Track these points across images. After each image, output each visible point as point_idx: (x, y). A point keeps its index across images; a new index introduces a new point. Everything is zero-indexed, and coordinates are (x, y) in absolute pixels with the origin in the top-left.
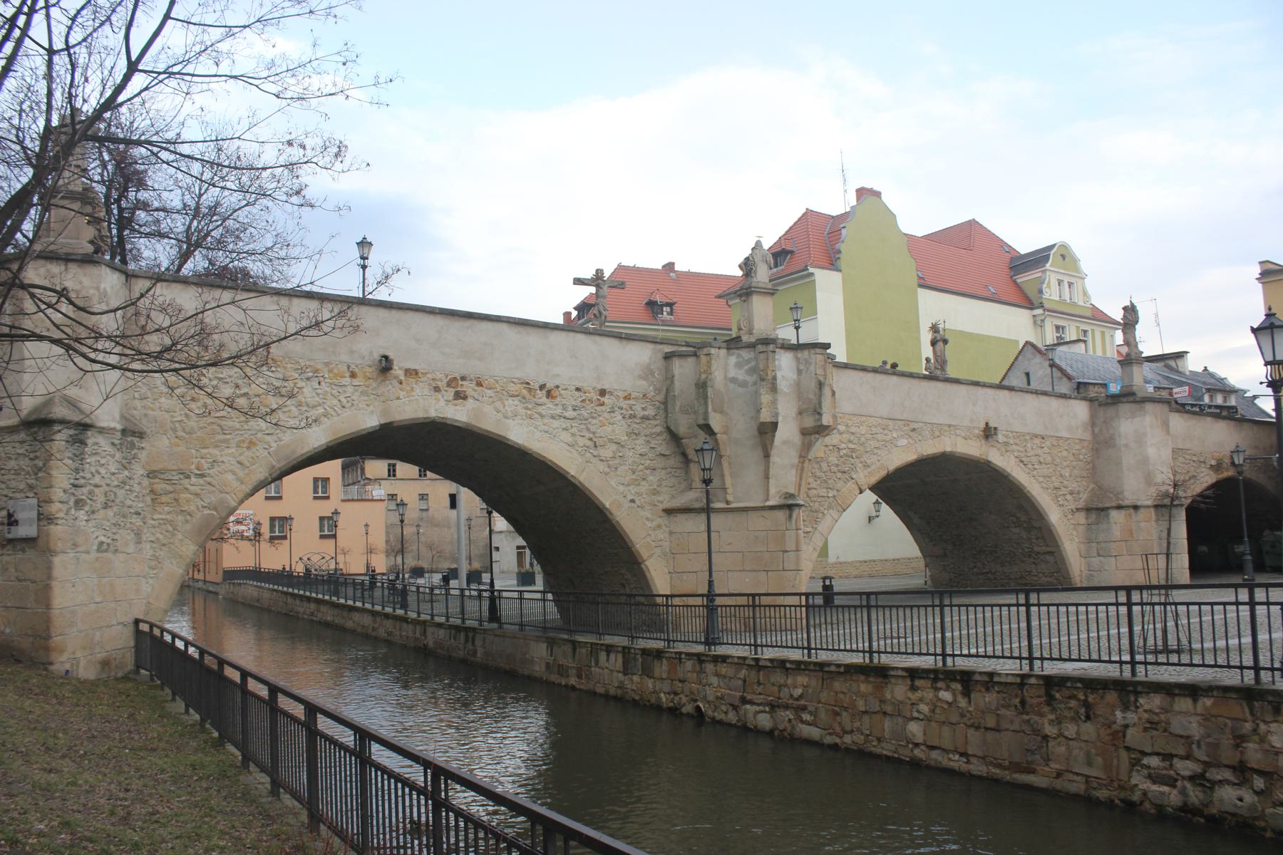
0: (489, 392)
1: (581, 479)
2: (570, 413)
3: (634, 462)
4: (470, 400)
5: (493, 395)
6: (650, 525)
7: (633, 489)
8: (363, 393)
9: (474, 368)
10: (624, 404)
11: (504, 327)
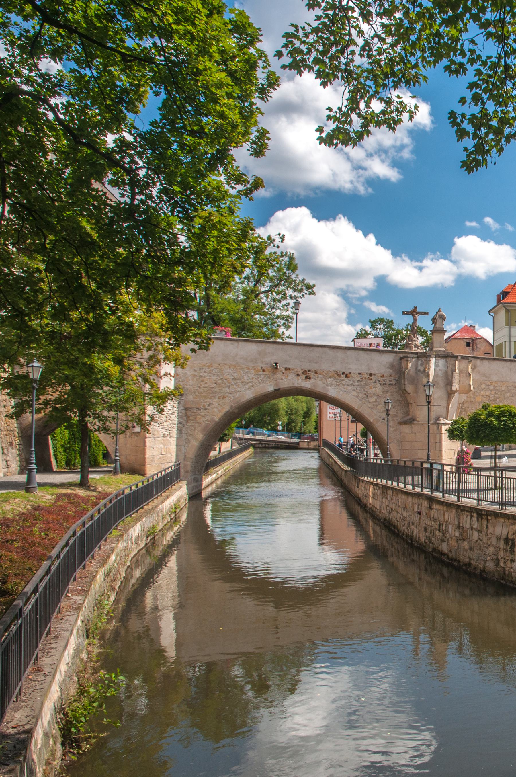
0: (320, 376)
1: (360, 410)
8: (268, 377)
9: (314, 366)
10: (381, 379)
11: (327, 349)
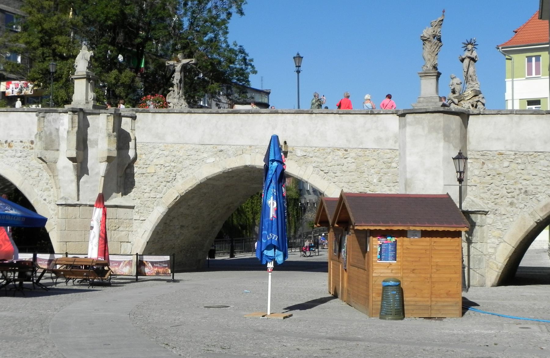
2: (19, 154)
3: (47, 179)
6: (53, 213)
7: (46, 193)
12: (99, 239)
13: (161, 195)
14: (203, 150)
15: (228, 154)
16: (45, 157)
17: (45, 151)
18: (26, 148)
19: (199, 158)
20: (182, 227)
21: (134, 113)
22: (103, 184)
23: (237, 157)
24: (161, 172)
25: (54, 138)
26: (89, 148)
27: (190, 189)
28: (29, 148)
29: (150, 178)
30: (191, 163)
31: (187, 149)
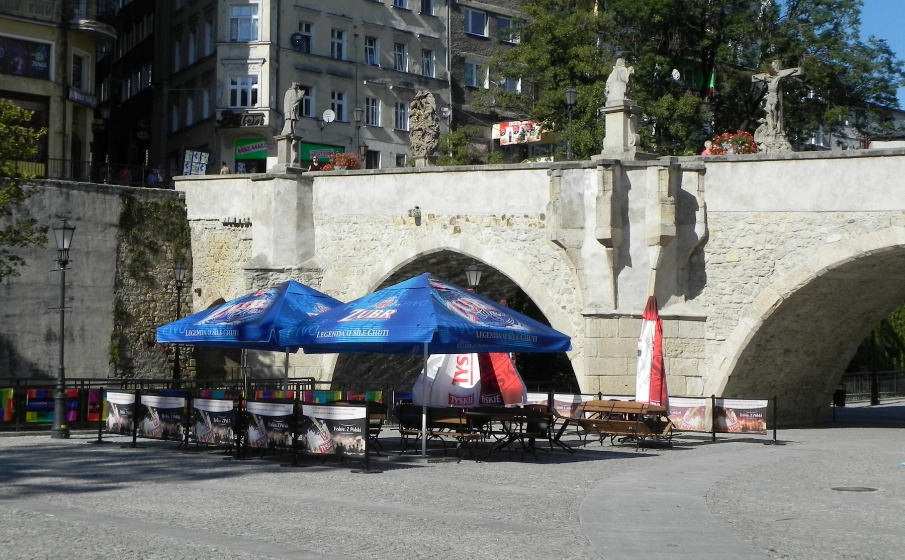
0: (474, 225)
2: (524, 236)
3: (566, 274)
4: (462, 233)
5: (475, 227)
6: (577, 328)
7: (565, 297)
8: (410, 234)
12: (651, 371)
13: (751, 298)
14: (820, 221)
15: (865, 228)
16: (563, 240)
17: (562, 230)
18: (533, 226)
19: (814, 234)
20: (787, 351)
21: (702, 163)
22: (654, 281)
23: (880, 232)
24: (749, 260)
25: (575, 208)
26: (631, 222)
27: (799, 287)
28: (538, 226)
29: (730, 269)
30: (801, 243)
31: (791, 221)
